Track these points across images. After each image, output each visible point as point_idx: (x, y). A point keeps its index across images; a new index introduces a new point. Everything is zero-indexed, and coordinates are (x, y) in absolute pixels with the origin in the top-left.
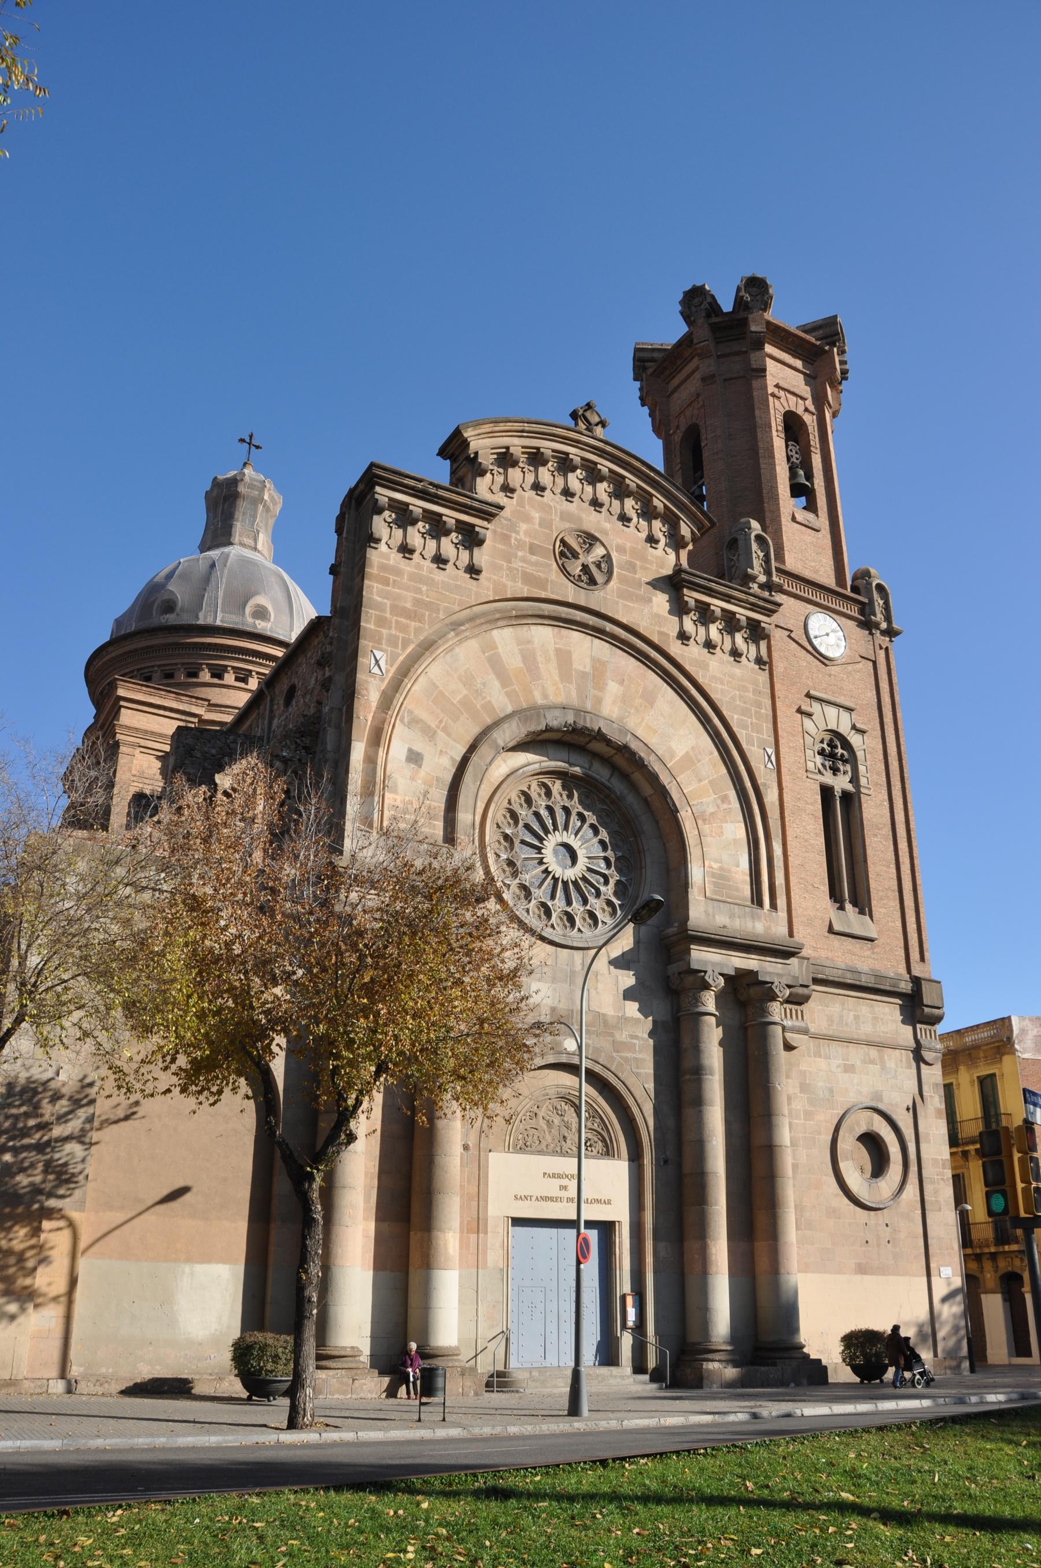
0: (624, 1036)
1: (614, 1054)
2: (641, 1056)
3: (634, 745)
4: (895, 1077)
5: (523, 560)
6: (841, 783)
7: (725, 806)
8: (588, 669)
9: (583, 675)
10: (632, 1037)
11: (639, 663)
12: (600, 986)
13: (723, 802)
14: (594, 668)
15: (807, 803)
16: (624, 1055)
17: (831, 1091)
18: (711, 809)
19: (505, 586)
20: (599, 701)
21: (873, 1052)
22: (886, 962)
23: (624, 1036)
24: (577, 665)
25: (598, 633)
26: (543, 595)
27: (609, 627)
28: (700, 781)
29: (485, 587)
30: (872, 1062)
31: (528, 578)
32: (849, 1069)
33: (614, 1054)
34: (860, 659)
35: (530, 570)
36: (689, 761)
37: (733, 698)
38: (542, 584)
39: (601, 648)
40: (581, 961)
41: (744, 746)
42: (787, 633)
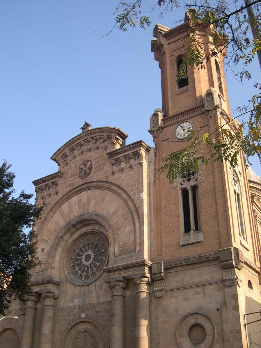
0: (99, 309)
1: (96, 315)
2: (104, 314)
3: (95, 217)
4: (211, 297)
5: (69, 181)
6: (188, 185)
7: (126, 221)
8: (86, 201)
9: (85, 203)
10: (101, 308)
11: (101, 190)
12: (93, 295)
13: (126, 220)
14: (88, 200)
15: (173, 200)
16: (99, 315)
17: (177, 310)
18: (122, 225)
19: (64, 191)
20: (88, 209)
21: (199, 290)
22: (209, 249)
23: (99, 309)
24: (83, 202)
25: (89, 188)
26: (73, 187)
27: (90, 185)
28: (118, 217)
29: (60, 195)
30: (198, 293)
31: (70, 185)
32: (186, 299)
33: (96, 315)
34: (201, 129)
35: (70, 182)
36: (115, 212)
37: (129, 183)
38: (73, 185)
39: (89, 193)
40: (87, 289)
41: (132, 197)
42: (167, 141)
